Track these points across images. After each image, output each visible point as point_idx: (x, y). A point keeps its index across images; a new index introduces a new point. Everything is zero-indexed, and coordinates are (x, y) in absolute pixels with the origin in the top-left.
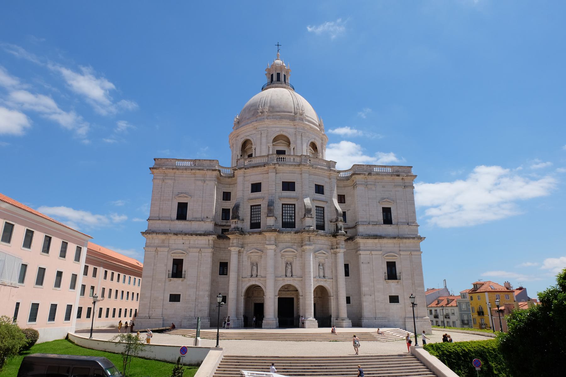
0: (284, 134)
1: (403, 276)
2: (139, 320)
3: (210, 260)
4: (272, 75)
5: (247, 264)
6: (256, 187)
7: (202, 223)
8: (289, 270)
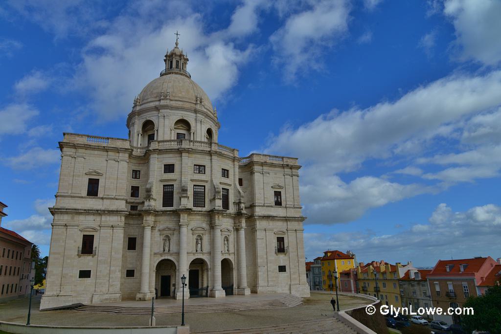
0: (185, 118)
1: (290, 249)
2: (46, 298)
3: (122, 235)
4: (171, 62)
5: (159, 239)
6: (169, 168)
8: (199, 245)
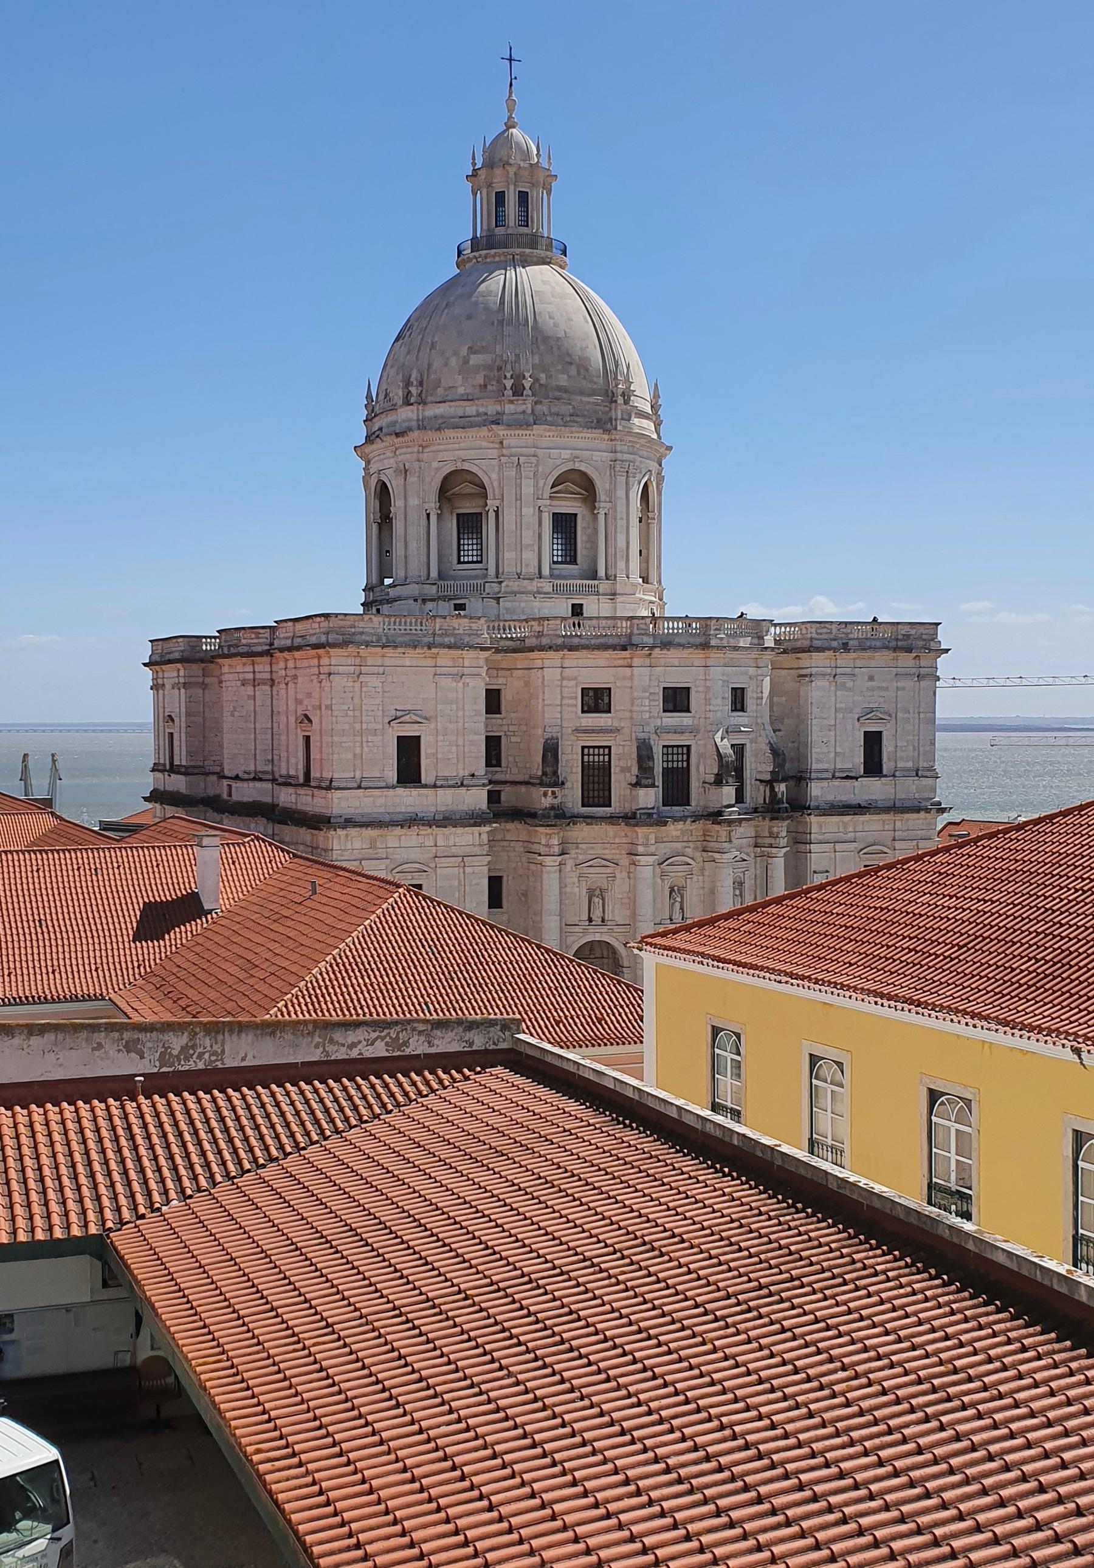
4: (500, 197)
7: (463, 790)
